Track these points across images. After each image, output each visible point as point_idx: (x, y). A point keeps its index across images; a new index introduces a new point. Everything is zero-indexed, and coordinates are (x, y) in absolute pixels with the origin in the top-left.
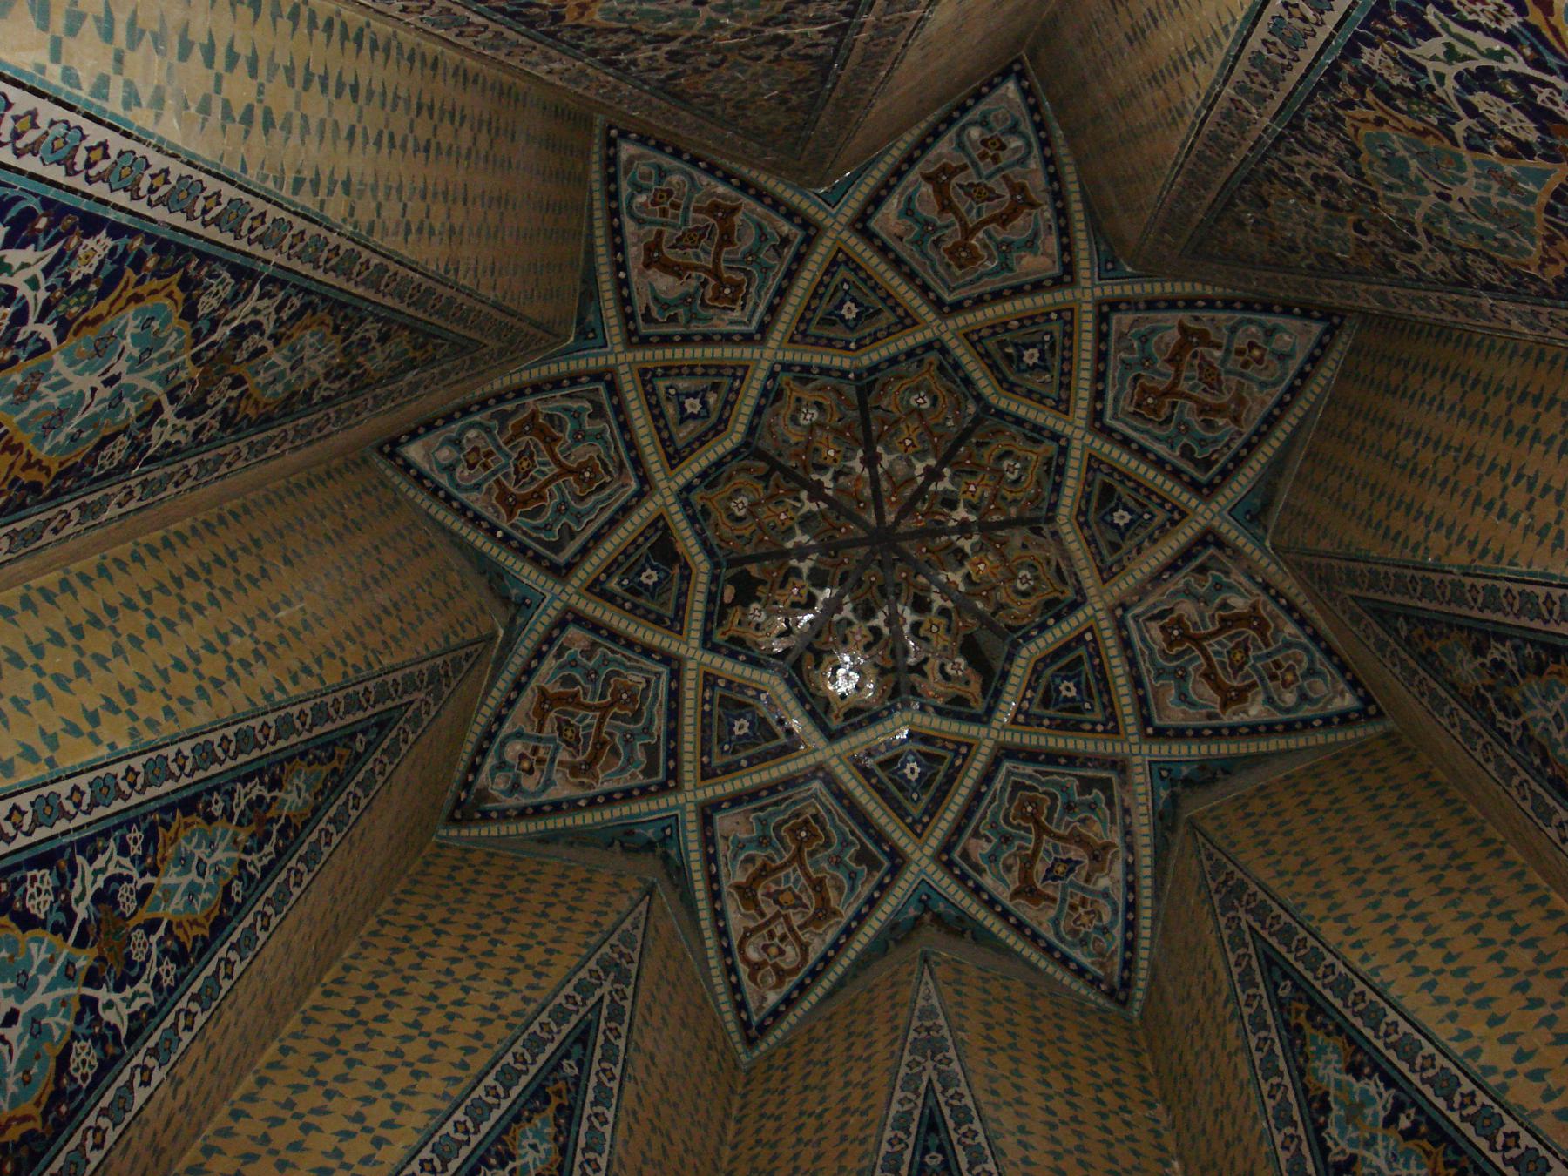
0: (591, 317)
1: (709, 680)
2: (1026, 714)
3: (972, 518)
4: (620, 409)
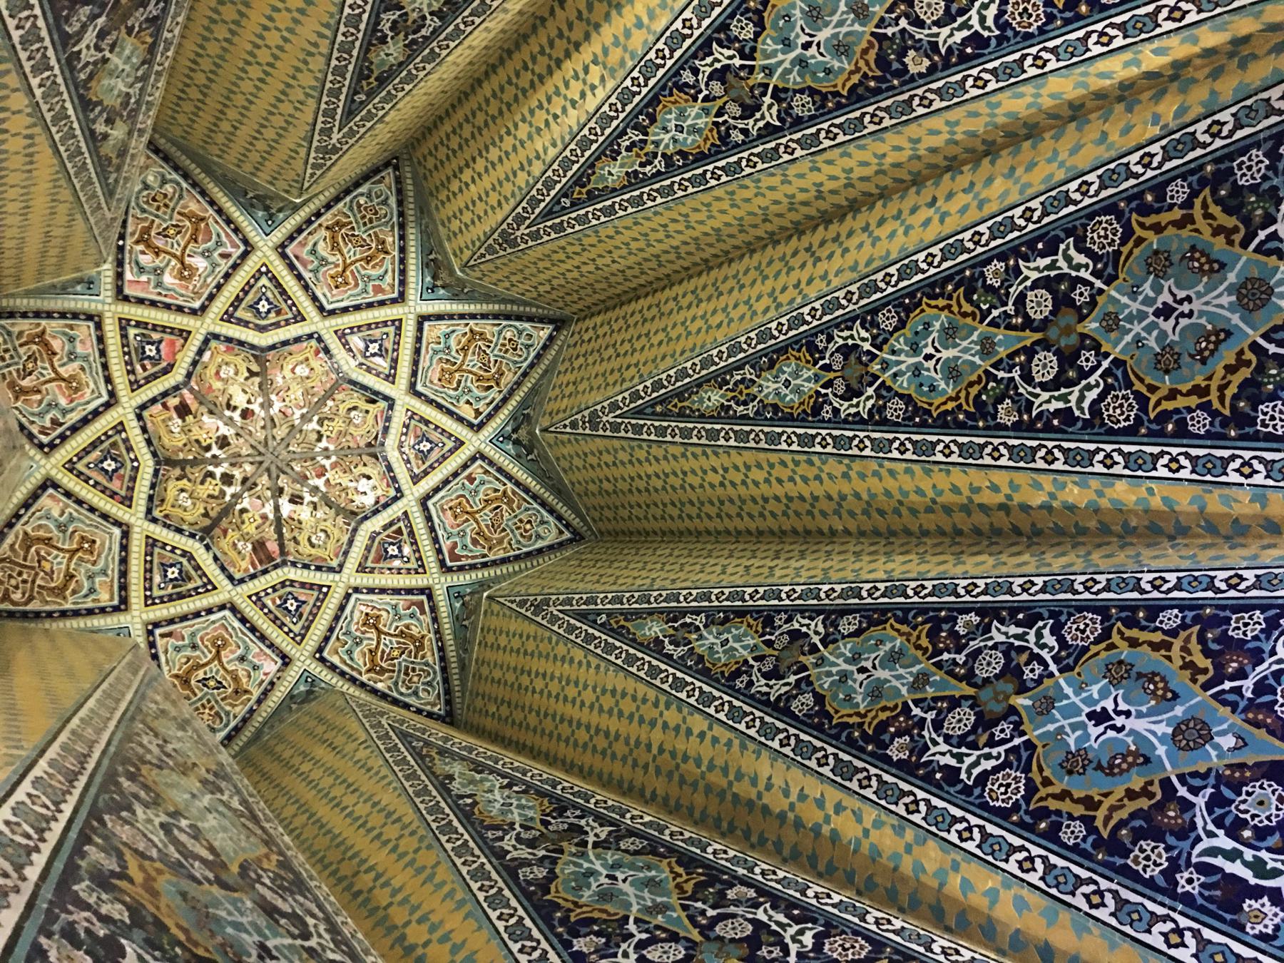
0: (281, 215)
1: (120, 428)
2: (259, 599)
3: (323, 489)
4: (235, 267)
